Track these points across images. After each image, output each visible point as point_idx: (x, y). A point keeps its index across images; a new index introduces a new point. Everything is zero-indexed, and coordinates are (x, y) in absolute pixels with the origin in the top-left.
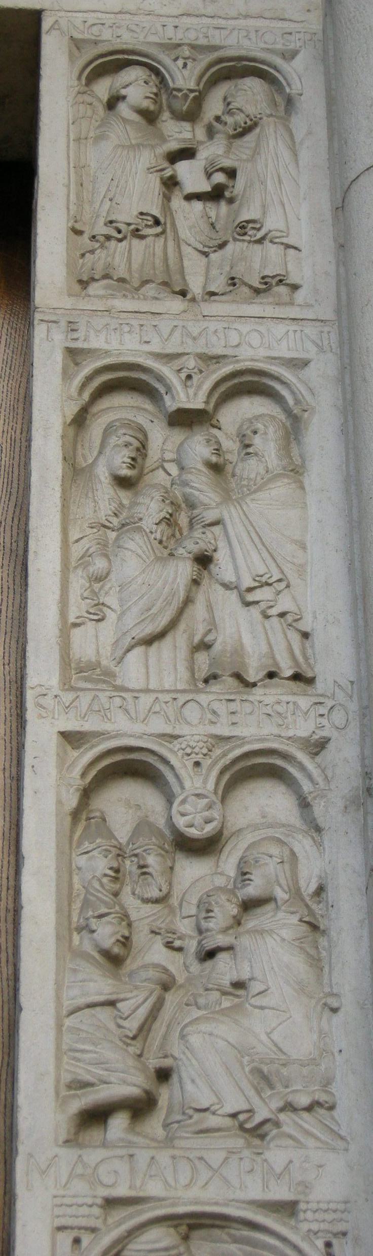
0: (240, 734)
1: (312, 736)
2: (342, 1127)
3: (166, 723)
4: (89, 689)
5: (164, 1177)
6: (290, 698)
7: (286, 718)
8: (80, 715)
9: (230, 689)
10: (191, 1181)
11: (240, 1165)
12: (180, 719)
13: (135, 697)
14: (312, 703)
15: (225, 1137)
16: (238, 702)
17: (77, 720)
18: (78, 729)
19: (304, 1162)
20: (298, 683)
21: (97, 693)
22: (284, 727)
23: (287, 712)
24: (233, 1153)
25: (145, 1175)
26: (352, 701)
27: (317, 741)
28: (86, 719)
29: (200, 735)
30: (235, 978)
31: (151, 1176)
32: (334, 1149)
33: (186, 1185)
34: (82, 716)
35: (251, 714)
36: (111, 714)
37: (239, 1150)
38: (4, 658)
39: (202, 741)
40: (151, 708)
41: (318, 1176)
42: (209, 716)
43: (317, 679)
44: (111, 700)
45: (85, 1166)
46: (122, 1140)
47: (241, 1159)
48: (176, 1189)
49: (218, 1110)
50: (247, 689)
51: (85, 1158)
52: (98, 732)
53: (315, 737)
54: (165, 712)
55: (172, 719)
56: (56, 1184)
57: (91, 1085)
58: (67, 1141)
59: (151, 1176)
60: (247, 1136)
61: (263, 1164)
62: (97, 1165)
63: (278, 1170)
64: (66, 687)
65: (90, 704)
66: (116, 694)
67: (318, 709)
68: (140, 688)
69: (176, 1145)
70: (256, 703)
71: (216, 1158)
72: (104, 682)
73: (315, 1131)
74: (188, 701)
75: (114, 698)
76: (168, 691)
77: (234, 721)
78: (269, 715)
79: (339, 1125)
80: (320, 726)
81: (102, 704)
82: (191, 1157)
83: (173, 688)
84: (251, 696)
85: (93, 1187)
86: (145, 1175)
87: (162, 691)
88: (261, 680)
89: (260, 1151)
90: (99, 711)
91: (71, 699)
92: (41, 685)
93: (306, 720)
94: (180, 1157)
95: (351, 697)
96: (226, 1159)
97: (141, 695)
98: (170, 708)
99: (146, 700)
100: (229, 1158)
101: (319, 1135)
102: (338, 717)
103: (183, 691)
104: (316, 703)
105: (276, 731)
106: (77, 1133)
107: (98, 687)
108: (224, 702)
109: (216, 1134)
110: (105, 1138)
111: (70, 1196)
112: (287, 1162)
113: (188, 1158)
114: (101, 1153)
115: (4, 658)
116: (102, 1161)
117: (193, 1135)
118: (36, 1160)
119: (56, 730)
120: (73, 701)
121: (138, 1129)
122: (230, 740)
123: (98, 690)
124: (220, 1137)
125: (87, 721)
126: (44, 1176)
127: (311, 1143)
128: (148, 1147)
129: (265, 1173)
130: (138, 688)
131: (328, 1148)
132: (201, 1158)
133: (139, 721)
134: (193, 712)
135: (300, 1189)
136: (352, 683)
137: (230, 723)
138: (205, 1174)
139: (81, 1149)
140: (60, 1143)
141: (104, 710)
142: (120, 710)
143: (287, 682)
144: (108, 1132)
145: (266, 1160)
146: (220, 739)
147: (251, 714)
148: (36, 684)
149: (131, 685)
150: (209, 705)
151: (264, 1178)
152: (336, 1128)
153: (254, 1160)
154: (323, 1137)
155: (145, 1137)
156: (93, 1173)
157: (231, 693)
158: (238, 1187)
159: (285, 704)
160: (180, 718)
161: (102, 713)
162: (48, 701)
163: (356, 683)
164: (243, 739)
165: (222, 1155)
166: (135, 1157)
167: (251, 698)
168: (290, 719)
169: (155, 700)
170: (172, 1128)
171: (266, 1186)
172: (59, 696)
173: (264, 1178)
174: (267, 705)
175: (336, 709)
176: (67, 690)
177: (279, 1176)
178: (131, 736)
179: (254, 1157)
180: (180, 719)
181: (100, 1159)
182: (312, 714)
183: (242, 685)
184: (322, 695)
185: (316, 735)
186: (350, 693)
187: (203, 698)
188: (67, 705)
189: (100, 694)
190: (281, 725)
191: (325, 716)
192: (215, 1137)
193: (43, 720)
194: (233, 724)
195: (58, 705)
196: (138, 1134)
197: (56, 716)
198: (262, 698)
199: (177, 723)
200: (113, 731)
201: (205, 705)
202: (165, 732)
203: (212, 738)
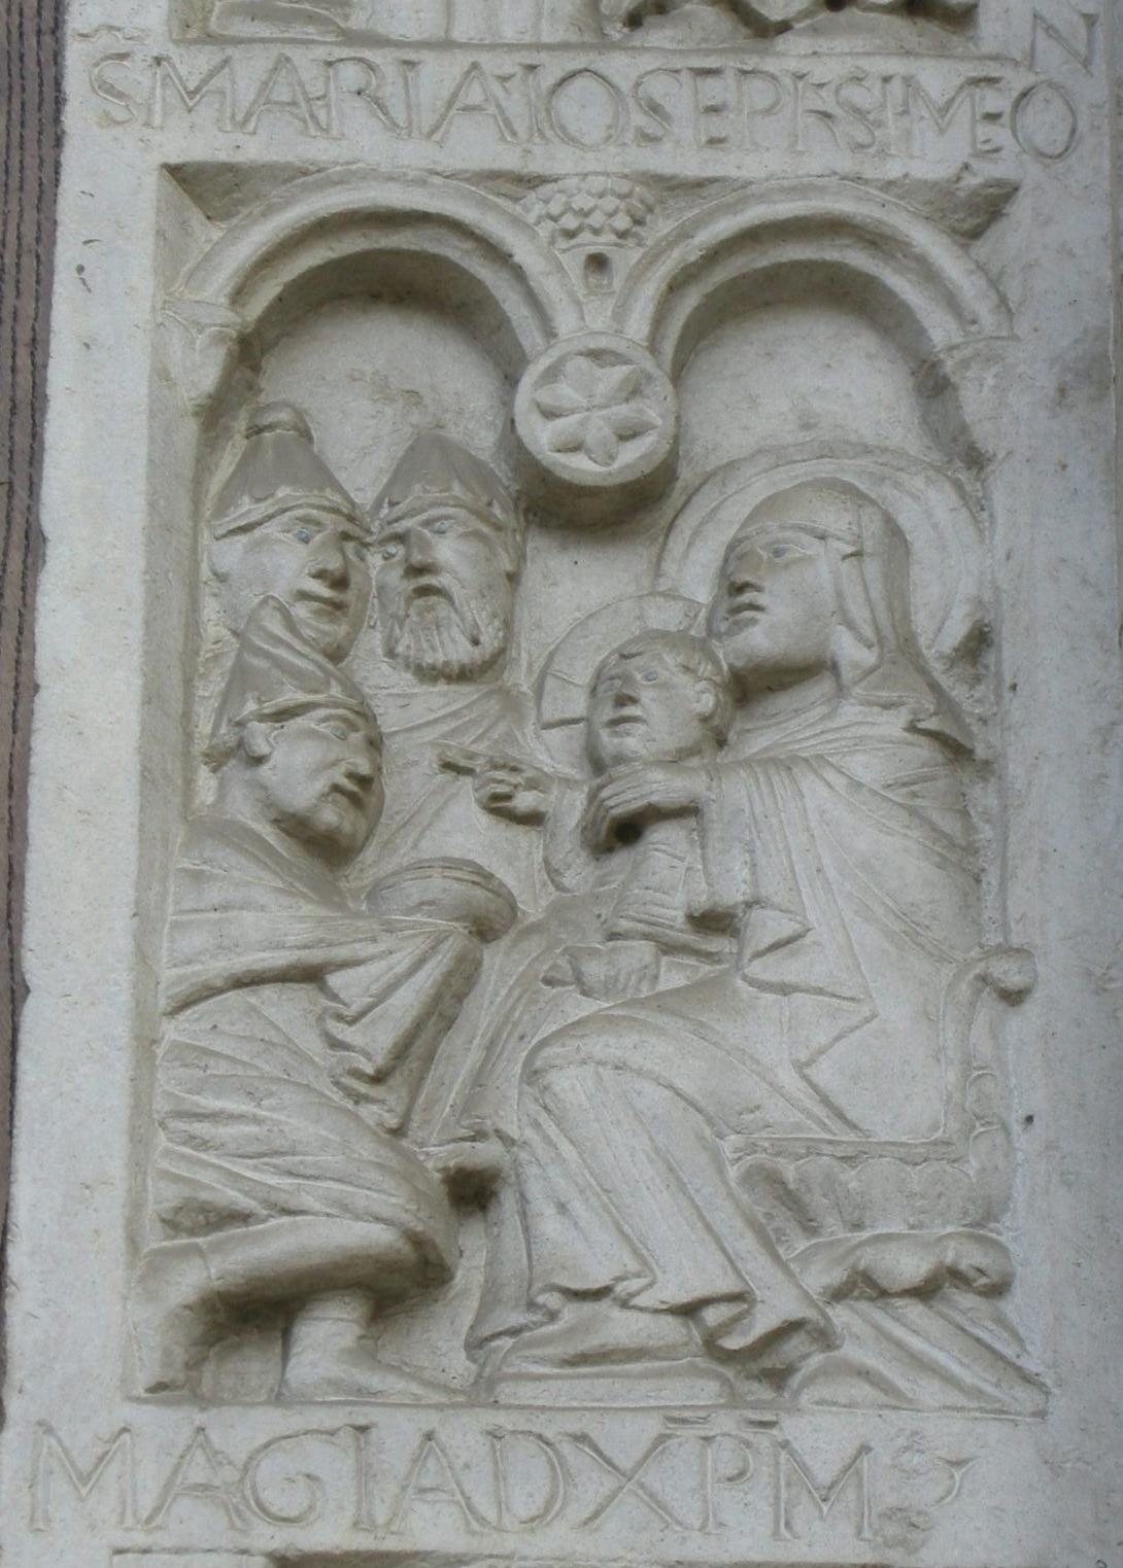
0: (733, 173)
1: (959, 179)
2: (1029, 1348)
3: (503, 139)
4: (263, 40)
5: (462, 1493)
6: (894, 65)
7: (879, 124)
8: (233, 116)
9: (706, 40)
10: (547, 1510)
11: (702, 1457)
12: (545, 126)
13: (406, 62)
14: (962, 79)
15: (661, 1374)
16: (730, 78)
17: (220, 129)
18: (223, 156)
19: (906, 1449)
20: (921, 22)
21: (288, 50)
22: (872, 150)
23: (883, 106)
24: (684, 1421)
25: (404, 1488)
26: (1090, 74)
27: (975, 193)
28: (251, 127)
29: (607, 174)
30: (702, 902)
31: (422, 1491)
32: (1001, 1412)
33: (532, 1520)
34: (240, 117)
35: (768, 111)
36: (329, 113)
37: (702, 1414)
38: (39, 14)
39: (613, 193)
40: (455, 95)
41: (949, 1493)
42: (638, 119)
43: (980, 10)
44: (331, 72)
45: (216, 1458)
46: (335, 1384)
47: (706, 1439)
48: (499, 1529)
49: (638, 1293)
50: (761, 44)
51: (215, 1437)
52: (286, 167)
53: (972, 181)
54: (499, 106)
55: (521, 128)
56: (123, 1515)
57: (245, 1218)
58: (160, 1387)
59: (422, 1491)
60: (729, 1373)
61: (777, 1456)
62: (251, 1458)
63: (824, 1476)
64: (193, 33)
65: (265, 84)
66: (346, 52)
67: (983, 99)
68: (425, 36)
69: (503, 1400)
70: (788, 81)
71: (627, 1438)
72: (311, 18)
73: (941, 1357)
74: (573, 75)
75: (341, 65)
76: (512, 47)
77: (716, 134)
78: (827, 115)
79: (1020, 1341)
80: (987, 147)
81: (301, 84)
82: (549, 1434)
83: (527, 39)
84: (768, 59)
85: (238, 1523)
86: (404, 1488)
87: (492, 47)
88: (807, 14)
89: (768, 1417)
90: (294, 103)
91: (205, 69)
92: (111, 28)
93: (942, 131)
94: (514, 1433)
95: (1086, 63)
96: (662, 1439)
97: (427, 56)
98: (516, 96)
99: (438, 75)
100: (669, 1436)
101: (955, 1368)
102: (1045, 123)
103: (565, 46)
104: (976, 82)
105: (846, 163)
106: (194, 1365)
107: (286, 35)
108: (685, 77)
109: (635, 1367)
110: (283, 1382)
111: (165, 1550)
112: (851, 1451)
113: (540, 1437)
114: (265, 1422)
115: (39, 14)
116: (267, 1445)
117: (556, 1371)
118: (59, 1441)
119: (157, 158)
120: (211, 75)
121: (388, 1356)
122: (705, 192)
123: (293, 41)
124: (644, 1375)
125: (254, 133)
126: (84, 1491)
127: (929, 1392)
128: (417, 1405)
129: (783, 1483)
130: (416, 37)
131: (981, 1410)
132: (581, 1438)
133: (415, 133)
134: (585, 109)
135: (892, 1530)
136: (1090, 20)
137: (704, 139)
138: (593, 1486)
139: (203, 1409)
140: (140, 1391)
141: (308, 100)
142: (358, 103)
143: (885, 18)
144: (292, 1362)
145: (785, 1445)
146: (672, 189)
147: (768, 111)
148: (95, 25)
149: (397, 30)
150: (638, 85)
151: (777, 1498)
152: (1009, 1351)
153: (748, 1444)
154: (968, 1377)
155: (416, 1376)
156: (242, 1480)
157: (708, 53)
158: (697, 1524)
159: (878, 84)
160: (549, 125)
161: (303, 110)
162: (135, 76)
163: (1101, 19)
164: (743, 187)
165: (653, 1426)
166: (374, 1433)
167: (770, 65)
168: (893, 128)
169: (468, 72)
170: (495, 1350)
171: (783, 1523)
172: (168, 59)
173: (777, 1498)
174: (821, 85)
175: (1038, 98)
176: (195, 41)
177: (827, 1493)
178: (391, 178)
179: (748, 1434)
180: (545, 126)
181: (262, 1440)
182: (962, 113)
183: (744, 30)
184: (995, 58)
185: (975, 175)
186: (1082, 49)
187: (620, 67)
188: (192, 86)
189: (297, 55)
190: (862, 146)
191: (1005, 119)
192: (627, 1375)
193: (117, 131)
194: (714, 142)
195: (163, 85)
196: (391, 1368)
197: (157, 120)
198: (803, 66)
199: (537, 140)
200: (336, 163)
201: (625, 86)
202: (496, 166)
203: (642, 183)
